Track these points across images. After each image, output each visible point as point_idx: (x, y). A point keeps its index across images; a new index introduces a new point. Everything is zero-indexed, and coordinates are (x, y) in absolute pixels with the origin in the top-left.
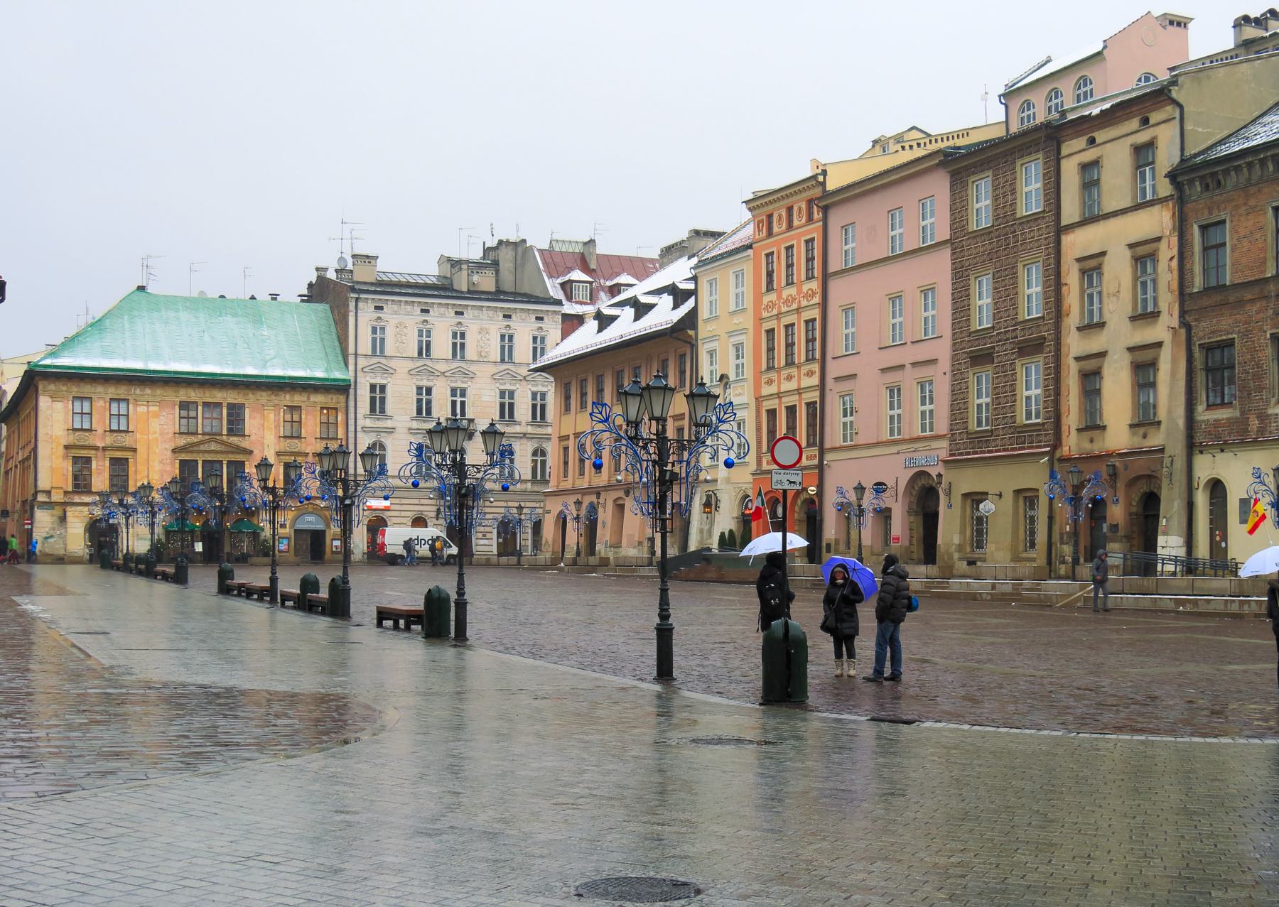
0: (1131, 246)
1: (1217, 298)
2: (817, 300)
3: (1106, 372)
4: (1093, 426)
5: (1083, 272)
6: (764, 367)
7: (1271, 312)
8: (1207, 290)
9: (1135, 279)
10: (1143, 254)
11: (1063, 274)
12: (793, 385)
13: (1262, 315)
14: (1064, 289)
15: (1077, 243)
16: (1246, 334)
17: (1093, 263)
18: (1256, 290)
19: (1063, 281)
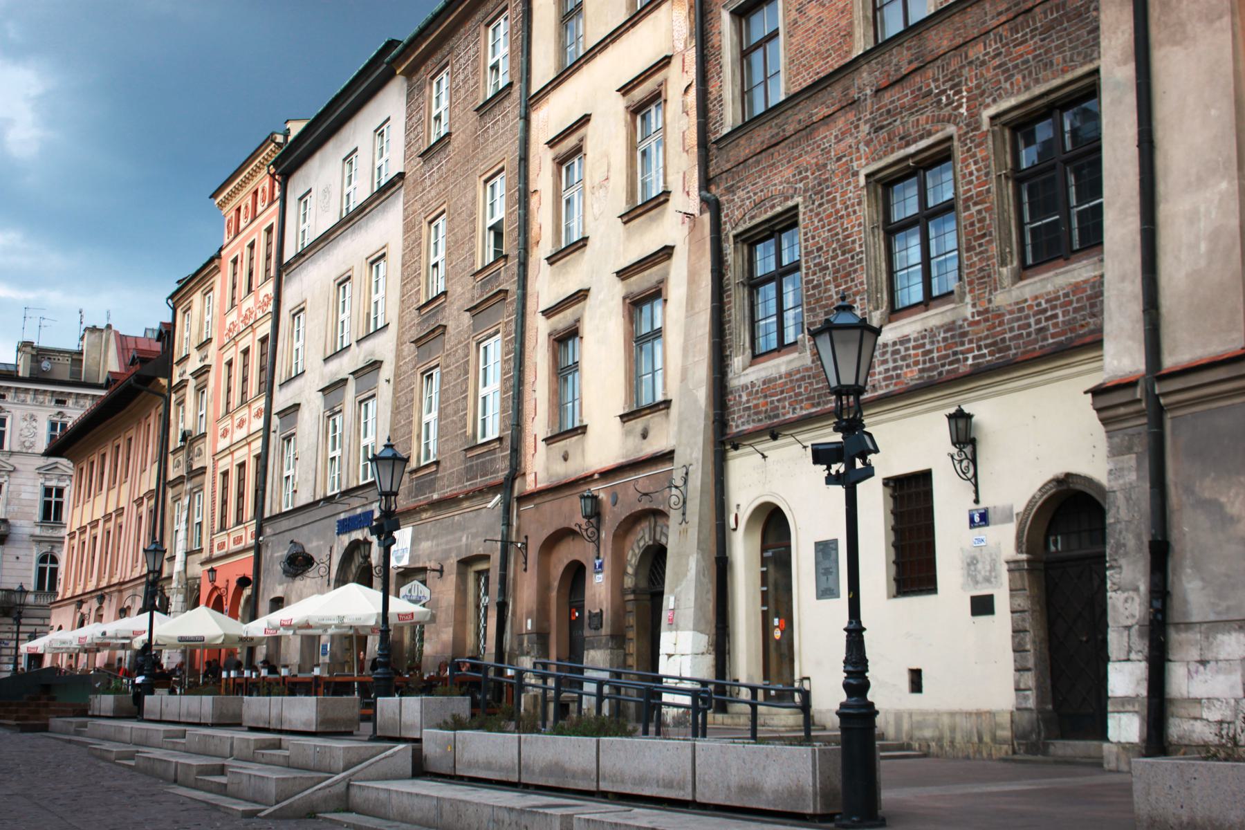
0: (625, 90)
1: (763, 135)
2: (270, 308)
3: (587, 329)
4: (567, 432)
5: (562, 161)
6: (222, 410)
7: (865, 128)
8: (748, 125)
9: (632, 147)
10: (642, 100)
11: (532, 176)
12: (240, 434)
13: (850, 140)
14: (534, 201)
15: (550, 118)
16: (820, 190)
17: (571, 141)
18: (836, 92)
19: (532, 188)
